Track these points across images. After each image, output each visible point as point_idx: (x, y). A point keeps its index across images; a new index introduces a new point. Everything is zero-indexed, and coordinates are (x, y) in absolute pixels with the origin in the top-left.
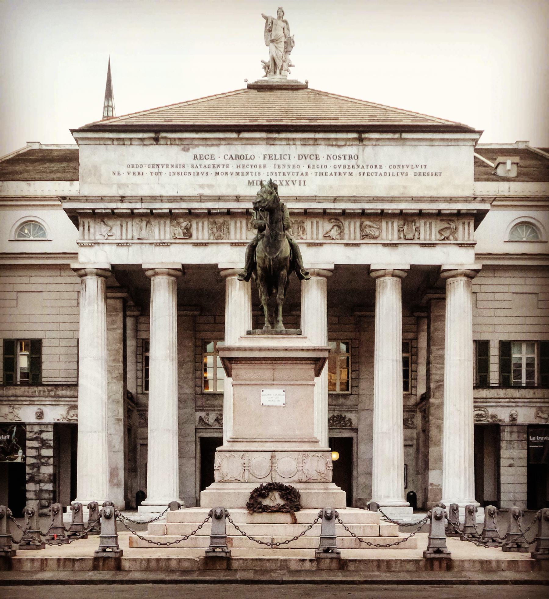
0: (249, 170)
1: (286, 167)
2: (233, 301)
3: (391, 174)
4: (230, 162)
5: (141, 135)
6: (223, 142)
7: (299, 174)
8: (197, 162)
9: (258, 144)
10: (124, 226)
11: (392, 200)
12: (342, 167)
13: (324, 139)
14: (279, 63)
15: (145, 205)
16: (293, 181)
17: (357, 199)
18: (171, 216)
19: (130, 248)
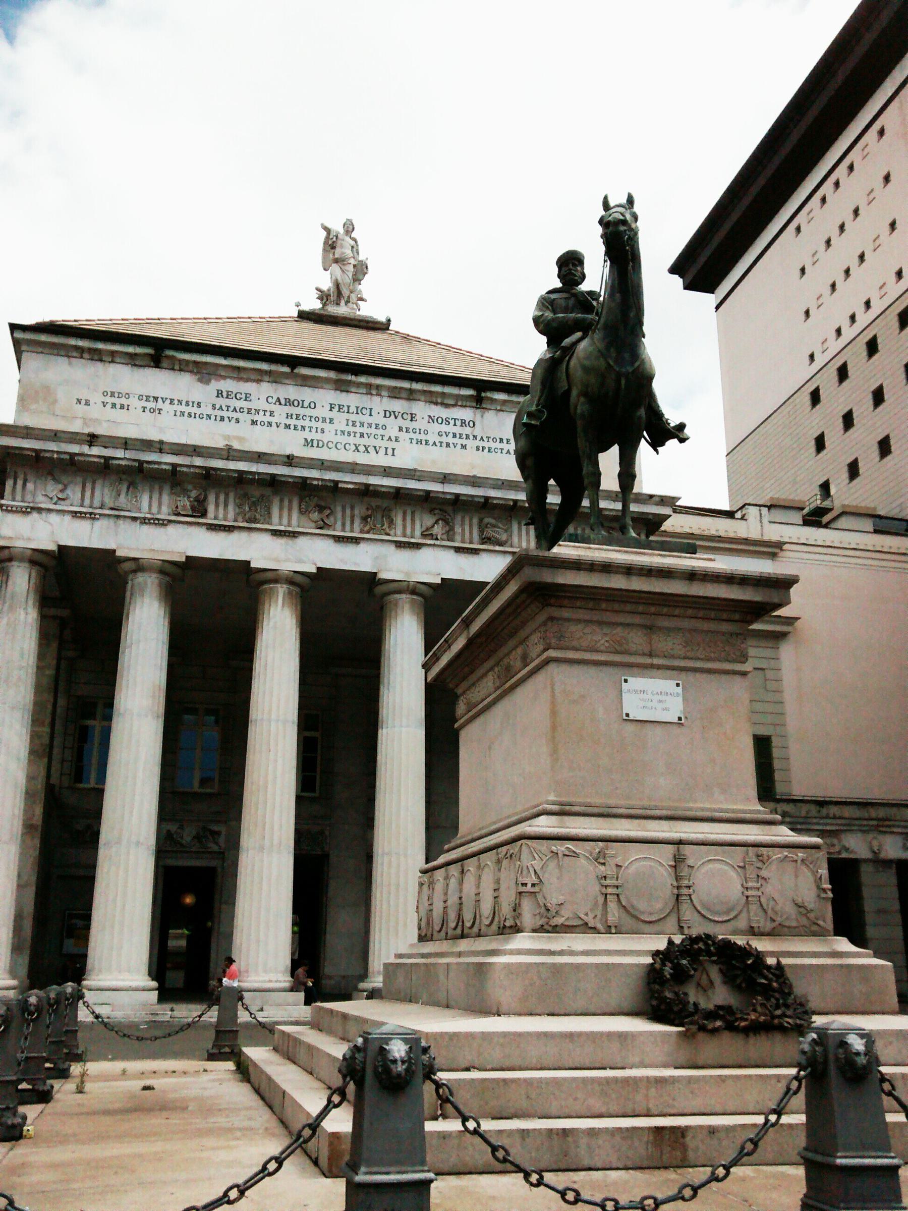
0: (307, 423)
1: (366, 425)
2: (271, 624)
4: (276, 408)
5: (130, 349)
6: (266, 378)
7: (386, 438)
8: (222, 402)
9: (322, 388)
10: (89, 486)
12: (451, 435)
13: (425, 391)
14: (345, 292)
15: (129, 454)
16: (375, 447)
17: (478, 480)
18: (173, 479)
19: (98, 524)
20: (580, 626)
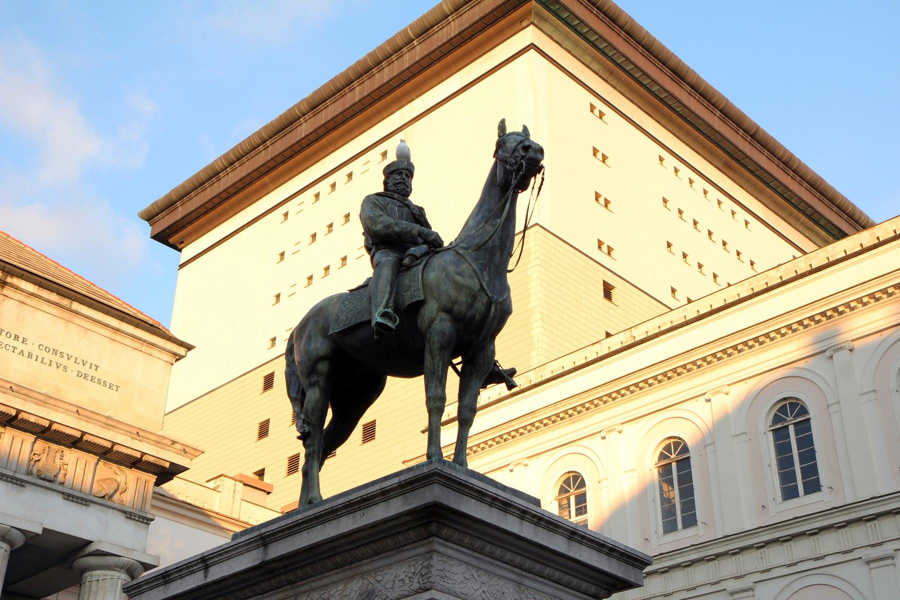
3: (40, 359)
11: (47, 400)
20: (462, 568)
